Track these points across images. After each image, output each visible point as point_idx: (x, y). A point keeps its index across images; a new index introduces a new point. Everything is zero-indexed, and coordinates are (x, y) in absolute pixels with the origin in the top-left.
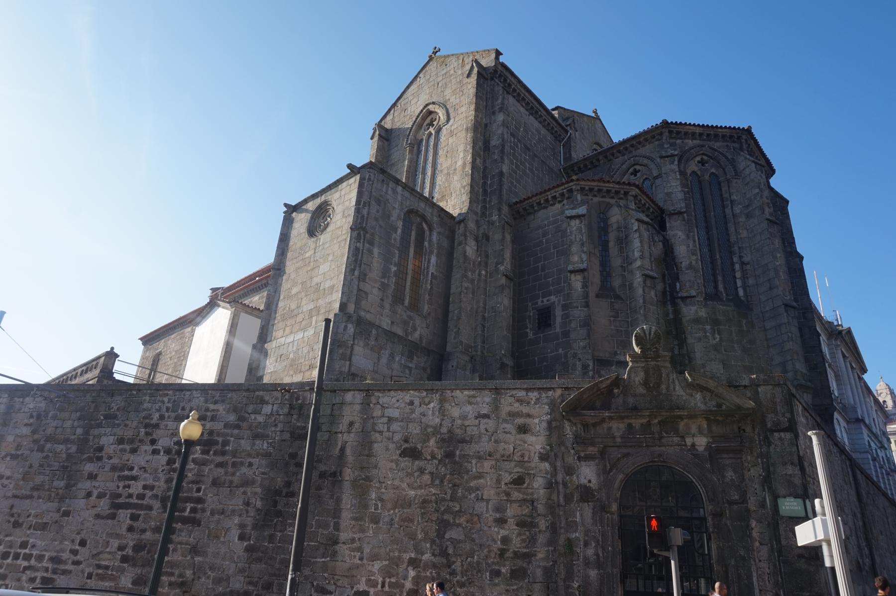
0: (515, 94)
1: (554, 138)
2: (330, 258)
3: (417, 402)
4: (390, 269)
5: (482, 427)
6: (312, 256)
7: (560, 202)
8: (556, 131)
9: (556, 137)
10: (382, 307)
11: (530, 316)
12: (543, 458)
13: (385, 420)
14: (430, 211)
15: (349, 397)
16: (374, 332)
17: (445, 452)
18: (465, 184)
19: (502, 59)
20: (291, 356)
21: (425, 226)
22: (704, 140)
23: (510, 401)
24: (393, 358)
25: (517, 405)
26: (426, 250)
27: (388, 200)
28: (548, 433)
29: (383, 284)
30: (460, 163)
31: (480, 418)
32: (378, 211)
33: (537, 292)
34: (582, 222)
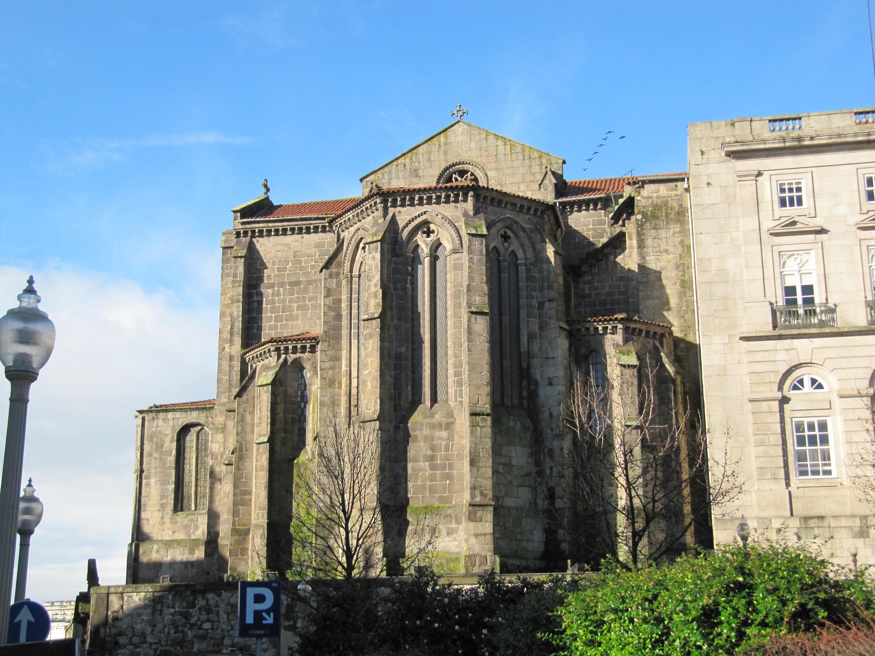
10: (163, 523)
14: (204, 415)
32: (152, 447)
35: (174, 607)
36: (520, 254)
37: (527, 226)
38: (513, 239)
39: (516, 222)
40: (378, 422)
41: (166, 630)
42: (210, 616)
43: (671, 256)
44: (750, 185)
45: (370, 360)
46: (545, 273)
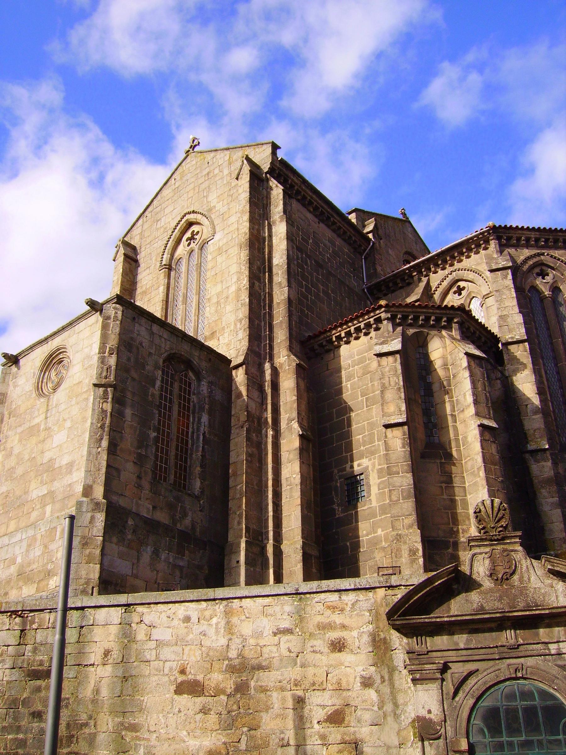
0: (299, 197)
1: (352, 250)
2: (68, 424)
3: (194, 619)
4: (148, 435)
5: (284, 647)
6: (43, 423)
7: (366, 334)
8: (355, 242)
9: (355, 249)
11: (337, 486)
12: (367, 683)
13: (153, 644)
15: (101, 615)
16: (130, 522)
17: (236, 684)
18: (241, 316)
19: (280, 155)
20: (19, 560)
21: (191, 374)
22: (542, 247)
23: (318, 608)
24: (157, 555)
25: (328, 612)
26: (194, 406)
27: (141, 344)
28: (371, 649)
29: (140, 456)
30: (233, 288)
31: (280, 633)
32: (129, 360)
33: (344, 454)
34: (396, 360)
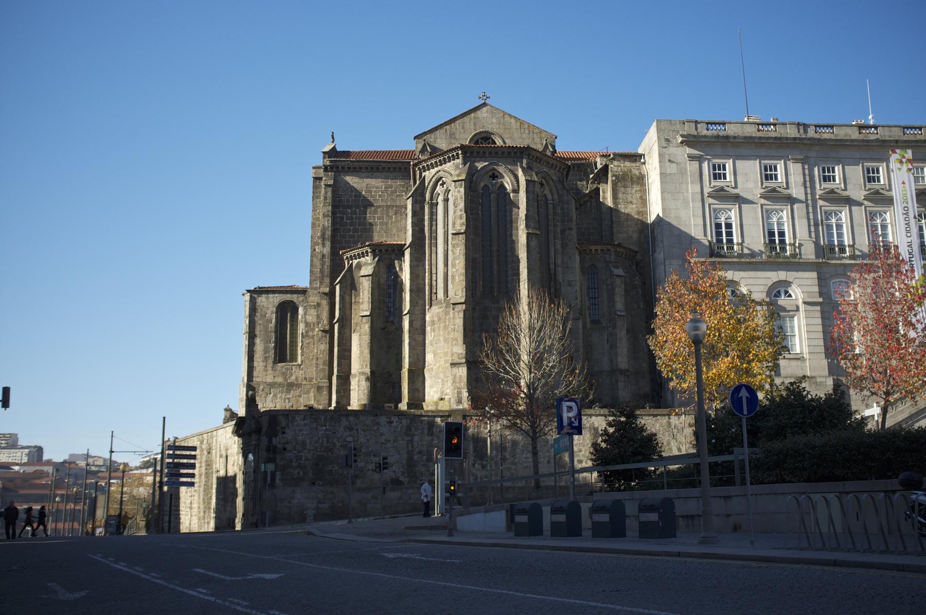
10: (266, 370)
27: (263, 306)
35: (325, 426)
36: (549, 196)
37: (554, 178)
38: (546, 187)
39: (549, 175)
40: (464, 306)
41: (321, 441)
42: (352, 432)
43: (634, 206)
44: (696, 164)
45: (457, 262)
46: (566, 210)
